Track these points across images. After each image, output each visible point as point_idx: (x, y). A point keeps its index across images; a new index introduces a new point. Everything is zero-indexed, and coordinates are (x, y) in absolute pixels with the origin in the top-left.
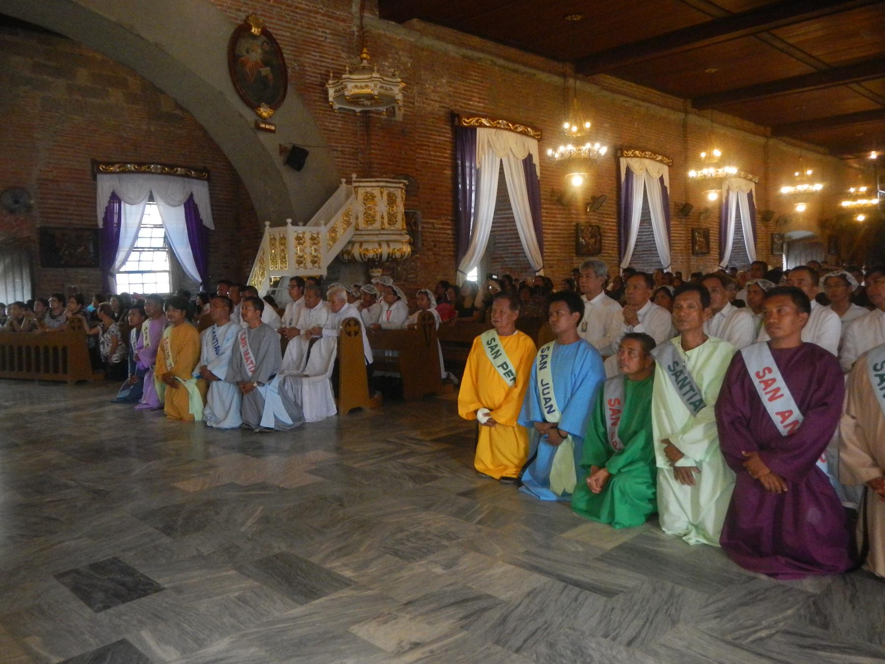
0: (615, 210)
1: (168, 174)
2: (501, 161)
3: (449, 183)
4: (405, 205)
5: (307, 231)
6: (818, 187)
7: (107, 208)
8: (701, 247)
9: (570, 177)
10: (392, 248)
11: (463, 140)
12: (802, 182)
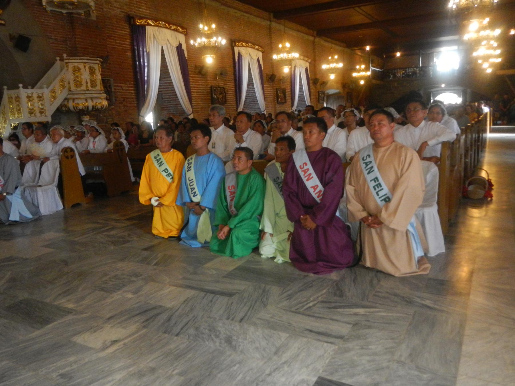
0: (233, 78)
2: (162, 47)
3: (130, 61)
4: (102, 75)
5: (35, 92)
6: (341, 65)
8: (281, 99)
10: (95, 102)
11: (138, 34)
12: (333, 62)
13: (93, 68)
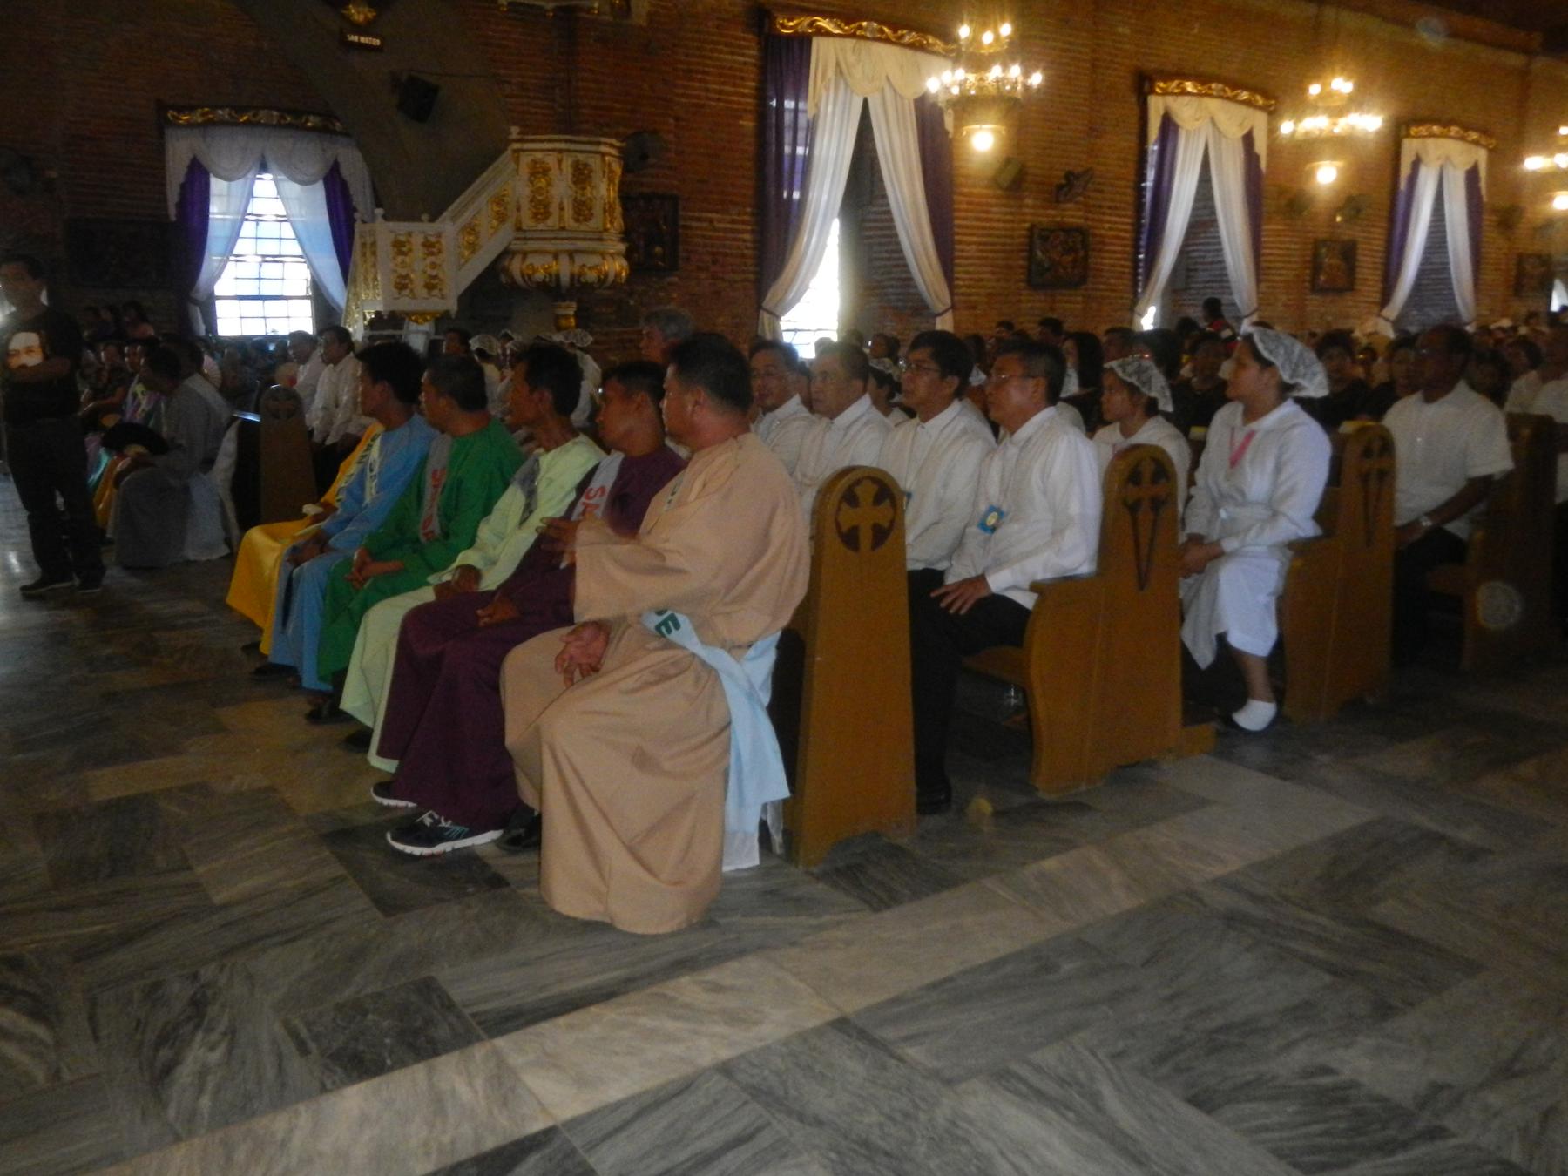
0: (1130, 199)
1: (290, 126)
2: (866, 102)
5: (419, 231)
7: (183, 186)
9: (969, 134)
11: (785, 63)
13: (586, 165)
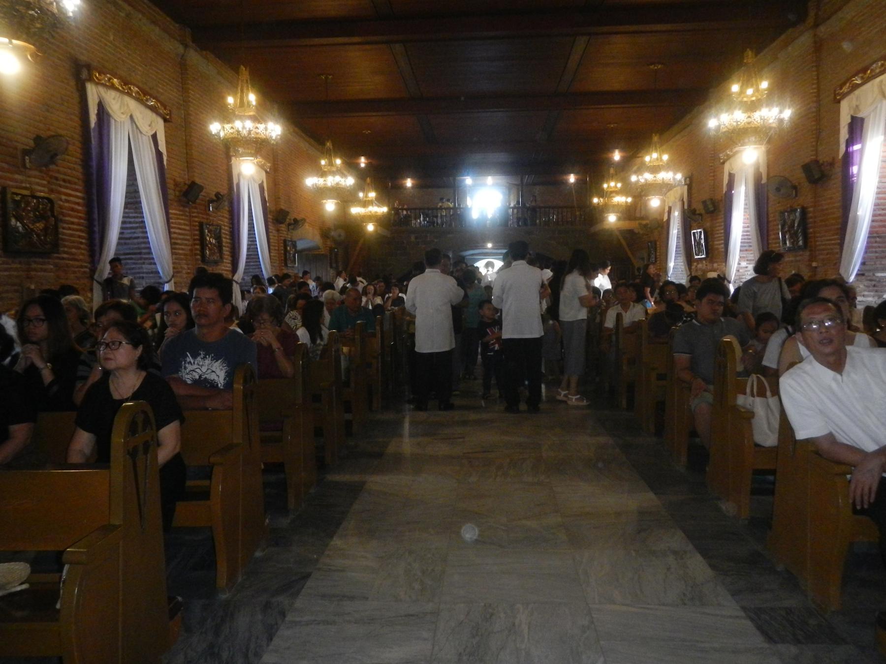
8: (212, 254)
12: (333, 173)
